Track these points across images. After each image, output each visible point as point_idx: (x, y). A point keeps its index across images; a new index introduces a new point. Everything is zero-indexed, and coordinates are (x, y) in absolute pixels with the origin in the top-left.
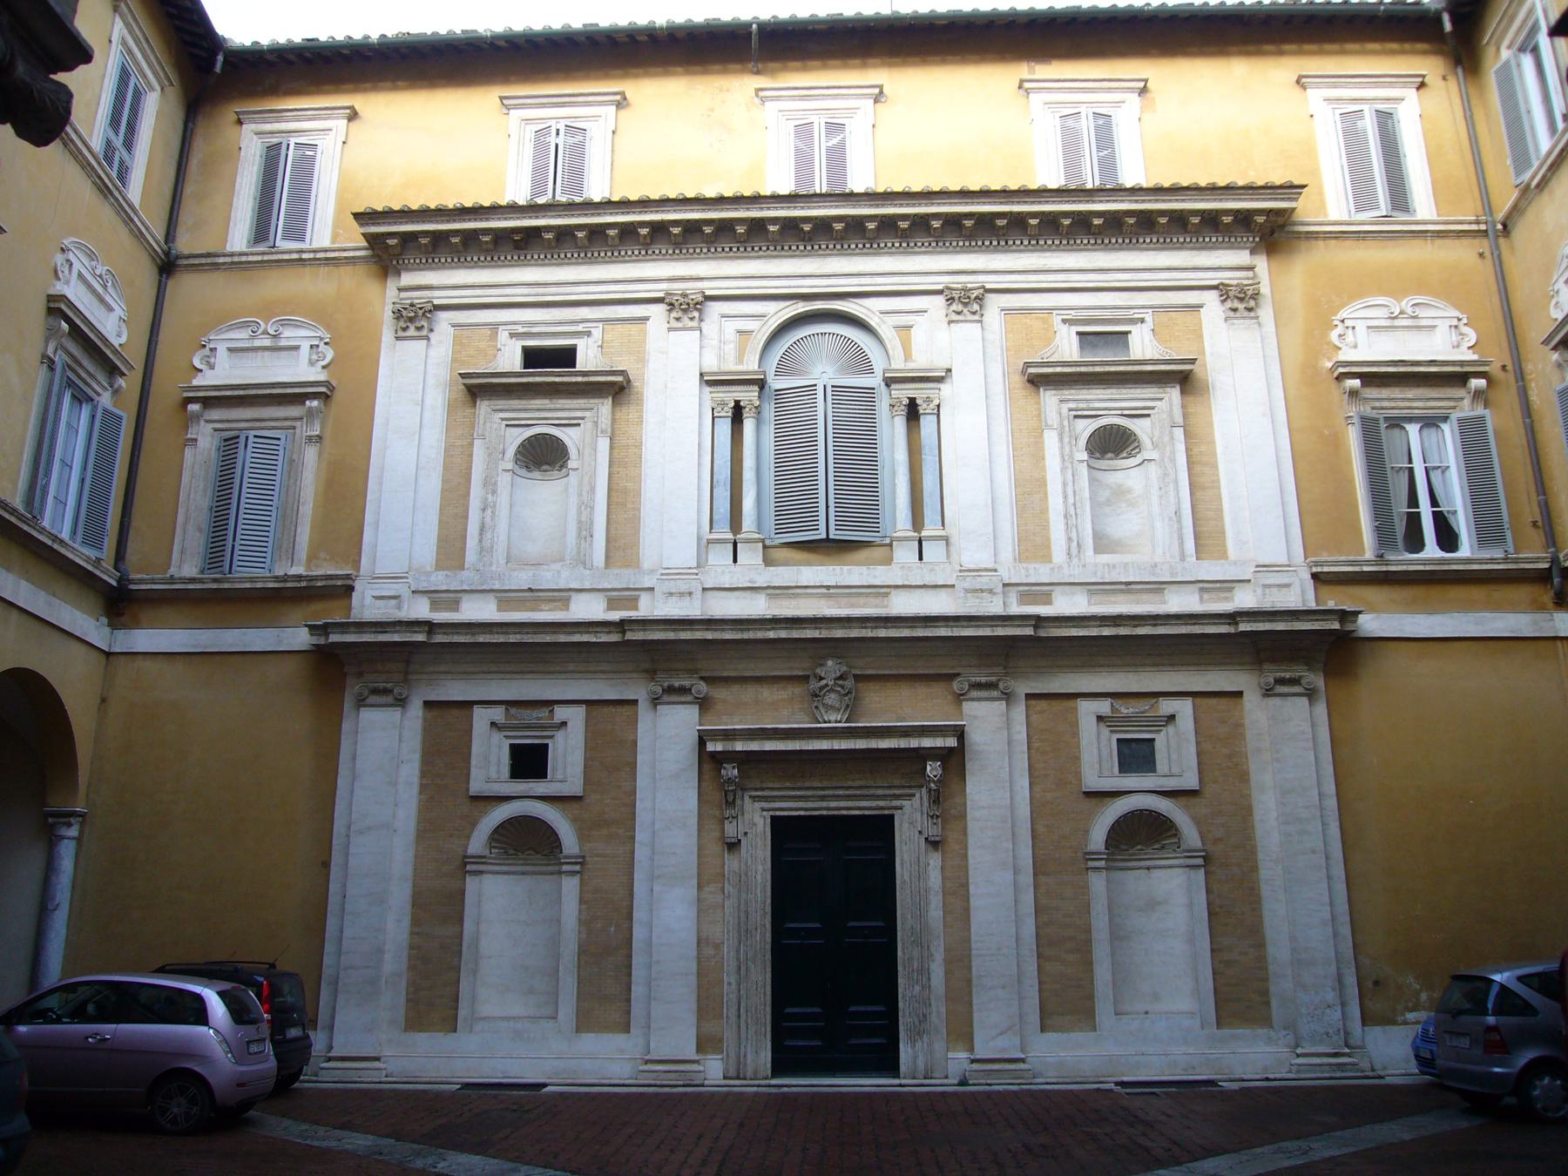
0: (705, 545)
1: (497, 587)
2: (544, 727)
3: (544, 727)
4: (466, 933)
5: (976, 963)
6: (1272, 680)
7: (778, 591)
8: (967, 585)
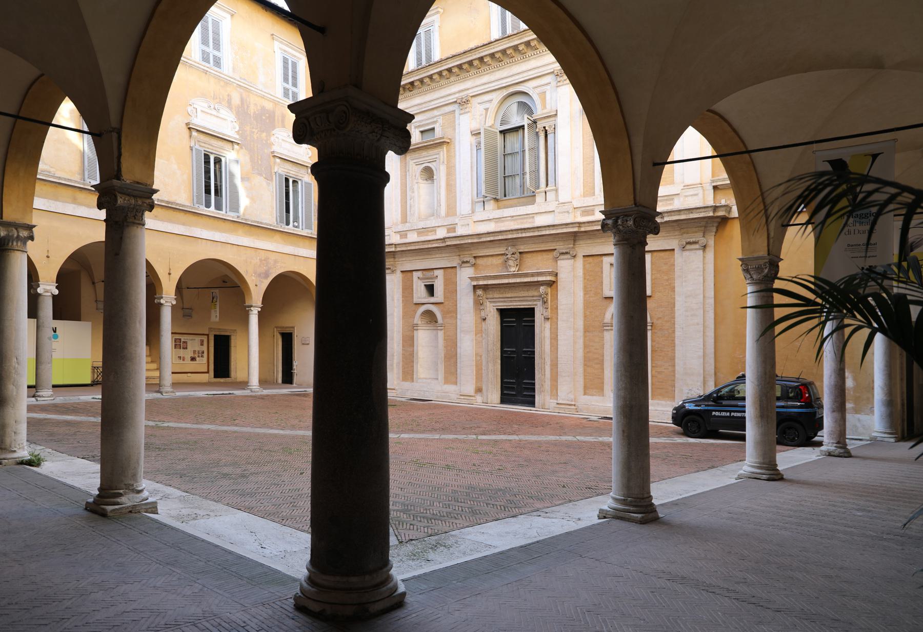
0: (473, 203)
1: (416, 228)
2: (431, 278)
3: (431, 278)
4: (415, 349)
5: (559, 366)
6: (685, 243)
8: (558, 210)
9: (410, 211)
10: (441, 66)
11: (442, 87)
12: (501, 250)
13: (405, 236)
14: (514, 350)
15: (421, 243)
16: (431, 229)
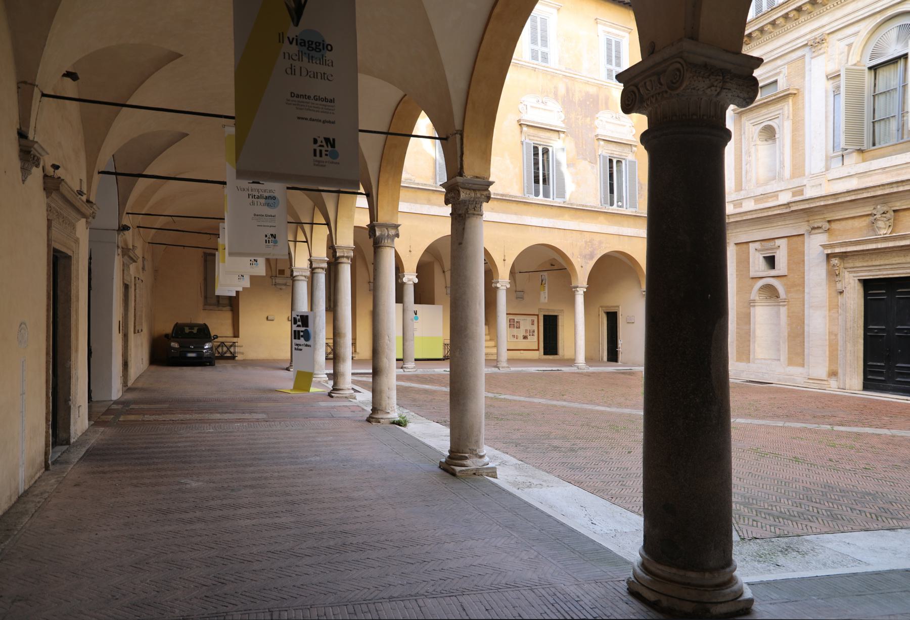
0: (828, 159)
1: (753, 196)
2: (772, 249)
3: (772, 249)
4: (751, 328)
7: (862, 175)
9: (746, 178)
10: (787, 7)
11: (787, 31)
12: (868, 210)
13: (741, 205)
14: (884, 327)
15: (760, 211)
16: (773, 194)
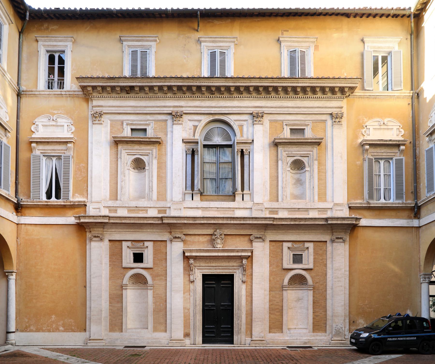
1: (127, 206)
2: (142, 248)
7: (204, 209)
9: (122, 191)
12: (210, 231)
13: (116, 211)
14: (214, 304)
15: (137, 219)
16: (143, 208)
